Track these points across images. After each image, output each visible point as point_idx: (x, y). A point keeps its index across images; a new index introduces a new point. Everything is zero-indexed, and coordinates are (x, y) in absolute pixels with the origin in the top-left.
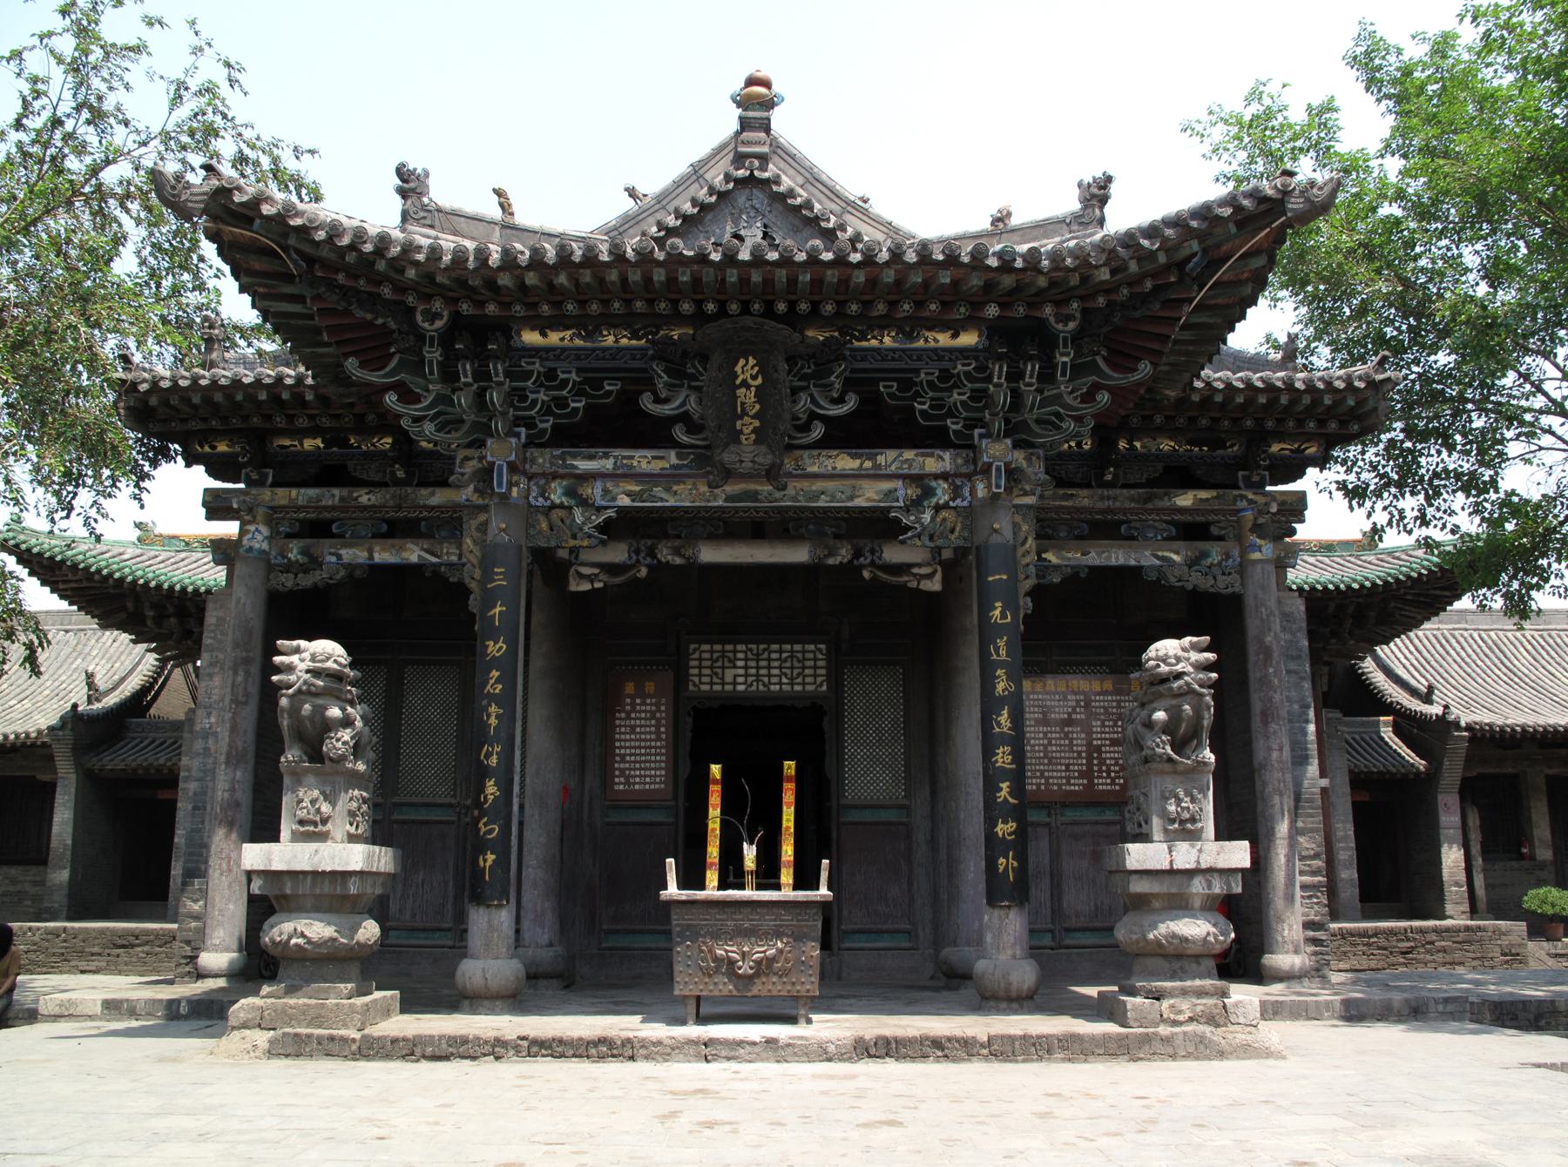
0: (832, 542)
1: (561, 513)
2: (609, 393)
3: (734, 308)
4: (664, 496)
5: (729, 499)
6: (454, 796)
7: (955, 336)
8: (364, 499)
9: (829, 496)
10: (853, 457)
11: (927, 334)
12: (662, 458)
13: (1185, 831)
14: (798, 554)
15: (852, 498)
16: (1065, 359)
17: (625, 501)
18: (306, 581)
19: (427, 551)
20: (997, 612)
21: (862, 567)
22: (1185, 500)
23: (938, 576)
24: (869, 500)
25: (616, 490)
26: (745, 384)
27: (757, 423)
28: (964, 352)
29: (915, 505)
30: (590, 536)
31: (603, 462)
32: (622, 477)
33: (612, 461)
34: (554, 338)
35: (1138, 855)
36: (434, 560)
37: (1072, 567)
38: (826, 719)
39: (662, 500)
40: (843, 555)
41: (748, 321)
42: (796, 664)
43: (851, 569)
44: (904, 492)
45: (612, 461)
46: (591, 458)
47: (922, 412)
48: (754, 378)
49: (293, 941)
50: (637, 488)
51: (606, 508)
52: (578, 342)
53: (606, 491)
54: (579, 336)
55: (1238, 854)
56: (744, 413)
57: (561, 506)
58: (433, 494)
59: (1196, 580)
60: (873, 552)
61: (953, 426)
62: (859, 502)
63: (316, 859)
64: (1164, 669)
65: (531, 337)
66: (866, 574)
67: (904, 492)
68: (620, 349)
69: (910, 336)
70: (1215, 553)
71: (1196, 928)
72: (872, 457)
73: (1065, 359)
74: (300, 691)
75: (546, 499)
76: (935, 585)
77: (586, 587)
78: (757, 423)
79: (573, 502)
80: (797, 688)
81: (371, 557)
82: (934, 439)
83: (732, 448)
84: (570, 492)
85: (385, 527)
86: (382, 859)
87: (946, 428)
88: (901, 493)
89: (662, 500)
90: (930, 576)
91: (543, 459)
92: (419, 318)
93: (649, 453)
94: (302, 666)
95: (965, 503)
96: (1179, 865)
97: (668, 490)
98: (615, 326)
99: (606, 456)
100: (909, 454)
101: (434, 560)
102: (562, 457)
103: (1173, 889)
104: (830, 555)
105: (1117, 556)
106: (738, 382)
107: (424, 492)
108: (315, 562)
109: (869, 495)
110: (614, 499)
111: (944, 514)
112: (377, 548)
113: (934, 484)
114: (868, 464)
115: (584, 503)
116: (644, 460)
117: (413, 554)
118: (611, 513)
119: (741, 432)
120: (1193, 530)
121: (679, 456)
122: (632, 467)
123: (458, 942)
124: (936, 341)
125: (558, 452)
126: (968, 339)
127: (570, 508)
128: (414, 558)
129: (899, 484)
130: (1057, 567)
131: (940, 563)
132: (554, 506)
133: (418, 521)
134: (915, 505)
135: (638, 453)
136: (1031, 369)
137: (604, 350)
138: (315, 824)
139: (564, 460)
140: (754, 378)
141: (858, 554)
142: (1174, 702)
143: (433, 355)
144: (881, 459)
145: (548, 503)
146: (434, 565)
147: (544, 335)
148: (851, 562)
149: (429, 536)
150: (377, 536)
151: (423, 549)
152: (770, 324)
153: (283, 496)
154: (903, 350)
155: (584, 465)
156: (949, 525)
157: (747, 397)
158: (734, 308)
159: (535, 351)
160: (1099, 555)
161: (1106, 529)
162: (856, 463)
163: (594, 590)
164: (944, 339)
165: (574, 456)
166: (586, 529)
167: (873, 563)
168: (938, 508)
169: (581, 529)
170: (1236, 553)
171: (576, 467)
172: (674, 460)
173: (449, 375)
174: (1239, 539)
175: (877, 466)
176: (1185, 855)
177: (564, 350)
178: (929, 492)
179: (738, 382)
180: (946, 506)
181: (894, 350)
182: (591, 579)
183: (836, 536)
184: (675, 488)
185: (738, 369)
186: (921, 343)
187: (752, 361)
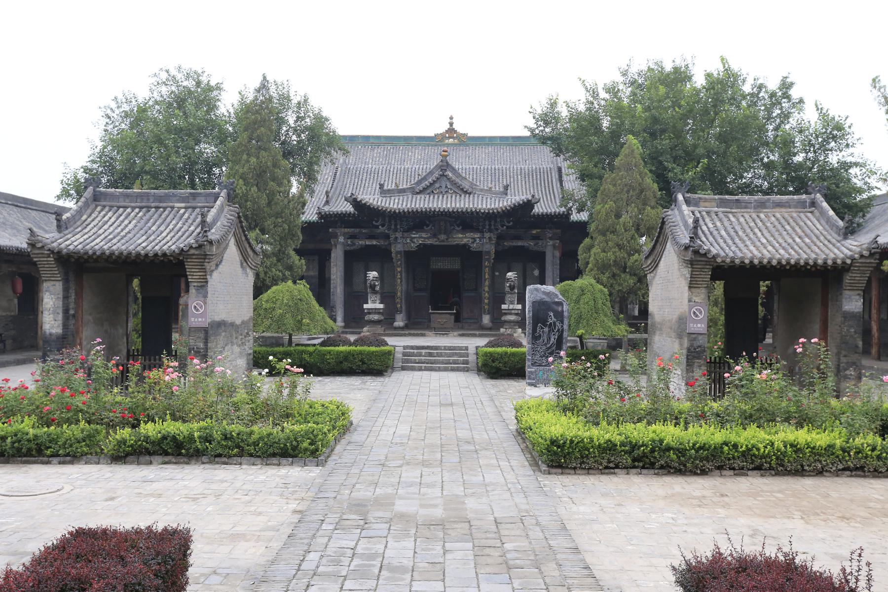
13: (512, 303)
18: (352, 248)
22: (534, 232)
35: (504, 307)
44: (471, 241)
55: (520, 307)
59: (536, 248)
67: (471, 241)
70: (540, 243)
71: (512, 318)
82: (476, 230)
86: (382, 306)
91: (406, 235)
103: (509, 312)
105: (520, 243)
108: (354, 244)
116: (424, 235)
117: (374, 242)
120: (536, 238)
123: (394, 320)
134: (473, 243)
136: (493, 223)
143: (387, 219)
153: (346, 230)
161: (518, 238)
173: (390, 221)
176: (511, 307)
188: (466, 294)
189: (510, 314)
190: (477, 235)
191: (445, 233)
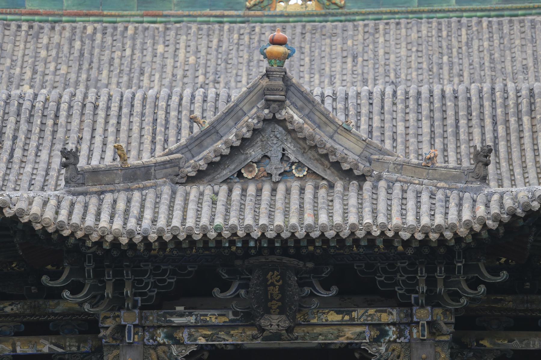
4: (226, 338)
12: (224, 315)
16: (459, 264)
19: (55, 345)
24: (348, 338)
31: (189, 318)
36: (60, 350)
39: (224, 340)
73: (459, 264)
79: (171, 342)
89: (224, 340)
101: (60, 350)
112: (18, 343)
119: (271, 308)
139: (165, 318)
151: (51, 343)
184: (232, 332)
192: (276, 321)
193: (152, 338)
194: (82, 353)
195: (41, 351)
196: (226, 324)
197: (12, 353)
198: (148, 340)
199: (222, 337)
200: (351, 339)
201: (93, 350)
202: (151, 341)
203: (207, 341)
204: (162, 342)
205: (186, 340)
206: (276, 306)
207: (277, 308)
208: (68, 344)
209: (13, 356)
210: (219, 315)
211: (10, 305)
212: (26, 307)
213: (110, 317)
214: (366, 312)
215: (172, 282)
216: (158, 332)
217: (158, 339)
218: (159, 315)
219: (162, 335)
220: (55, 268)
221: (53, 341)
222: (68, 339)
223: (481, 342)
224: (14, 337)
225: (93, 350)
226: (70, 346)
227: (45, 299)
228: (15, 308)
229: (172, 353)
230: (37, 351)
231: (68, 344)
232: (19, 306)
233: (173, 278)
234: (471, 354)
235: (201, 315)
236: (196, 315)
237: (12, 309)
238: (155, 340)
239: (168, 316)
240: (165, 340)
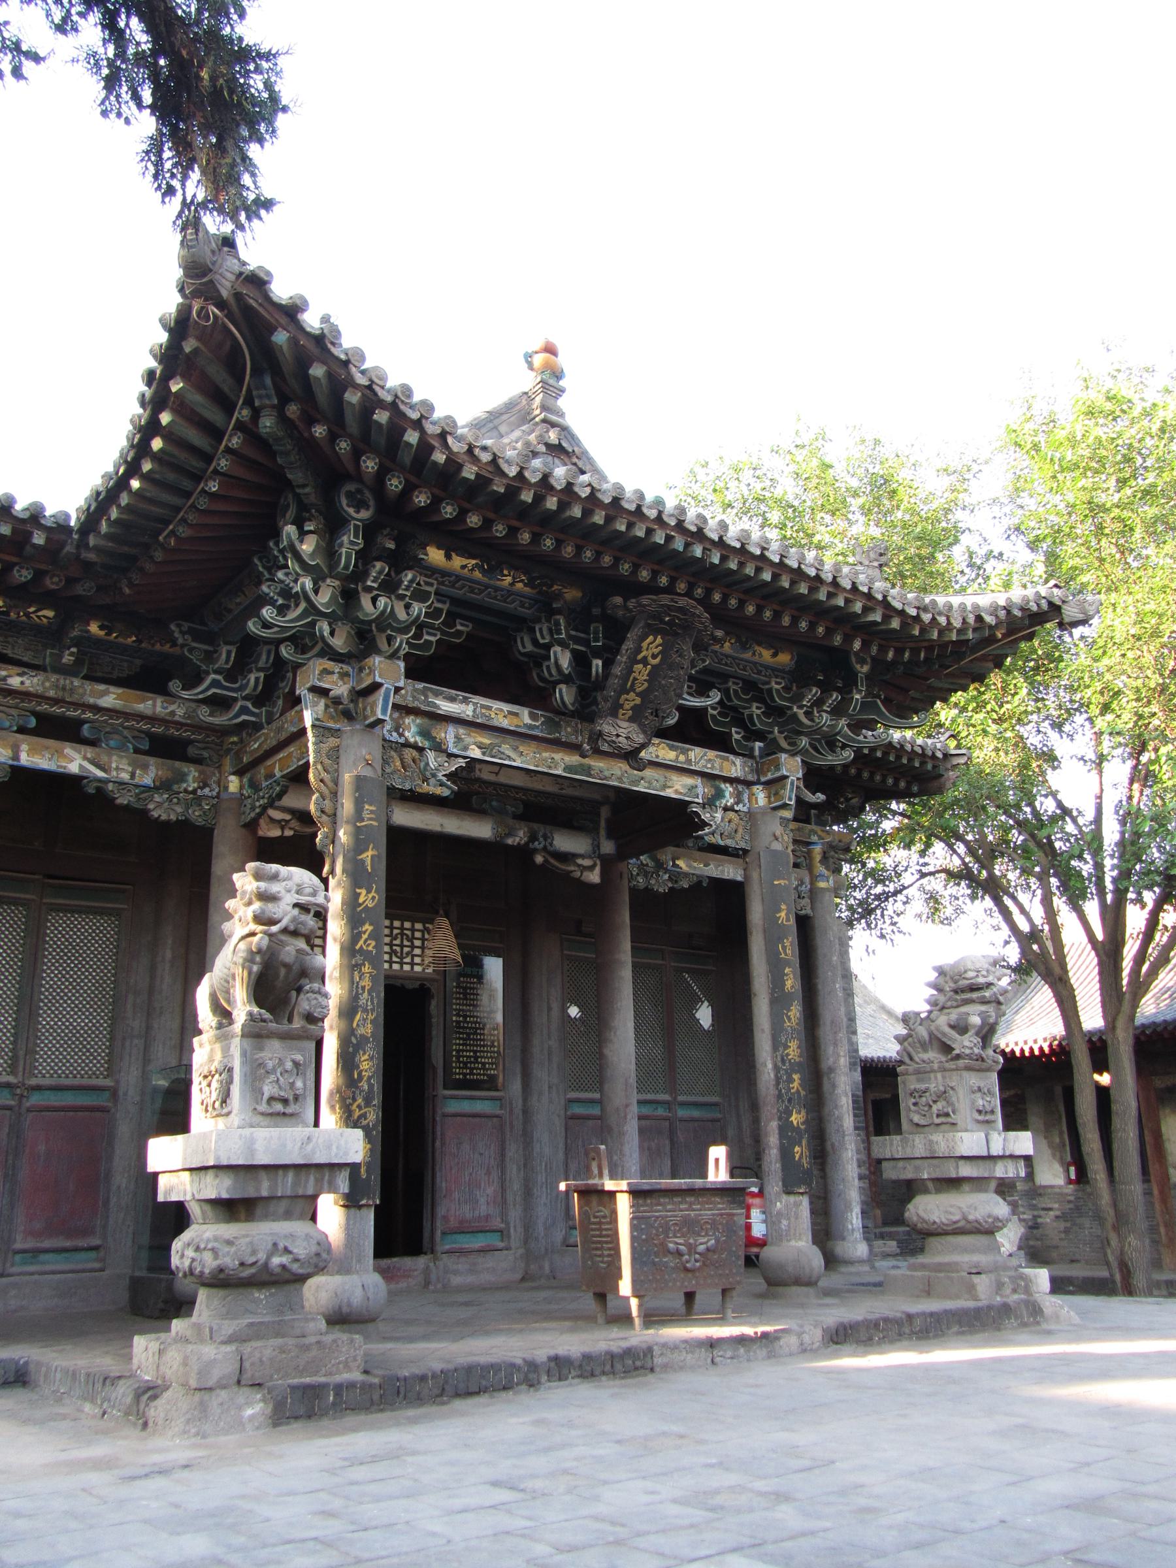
0: (511, 822)
1: (415, 753)
2: (459, 633)
3: (681, 587)
4: (513, 755)
5: (568, 768)
6: (13, 1072)
7: (775, 655)
8: (15, 682)
9: (648, 783)
10: (672, 748)
11: (757, 648)
12: (516, 714)
14: (481, 829)
15: (665, 787)
16: (858, 697)
17: (476, 753)
19: (92, 762)
20: (783, 914)
21: (535, 851)
23: (597, 870)
24: (677, 792)
25: (468, 740)
26: (644, 661)
27: (638, 701)
28: (776, 671)
29: (710, 803)
30: (442, 784)
31: (463, 707)
32: (481, 730)
33: (471, 707)
34: (457, 562)
36: (100, 774)
37: (698, 876)
38: (434, 1003)
39: (509, 758)
40: (519, 837)
41: (683, 602)
42: (406, 943)
43: (524, 853)
45: (471, 707)
46: (452, 699)
47: (713, 716)
48: (654, 656)
49: (276, 1260)
50: (487, 741)
51: (457, 756)
52: (477, 574)
53: (458, 739)
54: (479, 567)
56: (632, 689)
57: (415, 747)
58: (105, 693)
60: (545, 837)
61: (736, 735)
62: (669, 793)
63: (310, 1147)
64: (981, 980)
65: (435, 555)
66: (539, 859)
67: (702, 790)
68: (510, 593)
69: (744, 647)
72: (685, 752)
73: (858, 697)
74: (285, 931)
75: (401, 735)
76: (594, 877)
77: (276, 833)
78: (638, 701)
79: (427, 744)
80: (407, 968)
81: (16, 757)
83: (610, 720)
84: (425, 733)
85: (33, 723)
87: (730, 734)
88: (700, 790)
89: (509, 758)
90: (591, 868)
92: (344, 502)
93: (506, 707)
94: (290, 899)
95: (745, 809)
96: (994, 1153)
97: (515, 749)
98: (516, 569)
99: (465, 701)
100: (711, 754)
101: (100, 774)
102: (424, 692)
104: (509, 835)
106: (639, 657)
107: (88, 686)
109: (677, 787)
110: (466, 748)
111: (731, 814)
112: (24, 747)
113: (723, 786)
114: (682, 758)
115: (439, 748)
116: (500, 712)
118: (461, 762)
119: (621, 706)
121: (533, 716)
122: (489, 718)
124: (760, 655)
125: (420, 686)
126: (784, 658)
127: (421, 750)
128: (74, 768)
129: (698, 781)
130: (686, 875)
131: (601, 857)
132: (407, 745)
133: (81, 722)
134: (710, 803)
135: (496, 705)
137: (497, 589)
138: (285, 1101)
139: (426, 697)
140: (654, 656)
141: (533, 838)
142: (983, 1008)
144: (692, 755)
145: (402, 740)
146: (100, 780)
147: (448, 557)
148: (527, 844)
149: (92, 743)
150: (22, 730)
151: (85, 758)
152: (699, 610)
154: (734, 658)
155: (446, 707)
156: (733, 825)
157: (641, 673)
158: (681, 587)
159: (432, 571)
160: (716, 867)
162: (672, 755)
163: (282, 838)
164: (766, 655)
165: (437, 694)
166: (440, 775)
167: (545, 848)
168: (726, 809)
169: (434, 776)
170: (807, 880)
171: (438, 707)
172: (527, 720)
174: (810, 868)
175: (689, 761)
177: (459, 578)
178: (719, 794)
179: (639, 657)
180: (731, 809)
181: (727, 656)
182: (282, 824)
183: (516, 817)
184: (521, 749)
185: (645, 645)
186: (747, 655)
187: (659, 640)
188: (453, 1107)
189: (978, 1183)
190: (736, 767)
191: (636, 716)
192: (626, 731)
193: (397, 730)
194: (137, 786)
195: (65, 768)
196: (519, 730)
197: (11, 762)
198: (390, 732)
199: (507, 752)
200: (681, 793)
201: (158, 784)
202: (395, 734)
203: (484, 754)
204: (412, 740)
205: (451, 745)
206: (632, 704)
207: (632, 709)
208: (114, 765)
209: (11, 766)
210: (510, 713)
211: (19, 675)
212: (47, 684)
213: (333, 673)
214: (705, 755)
215: (431, 642)
216: (407, 721)
217: (407, 734)
218: (416, 690)
219: (414, 729)
220: (102, 633)
221: (89, 755)
222: (115, 758)
223: (677, 862)
224: (18, 735)
225: (158, 784)
226: (117, 769)
227: (86, 678)
228: (28, 683)
229: (427, 764)
230: (58, 766)
231: (114, 765)
232: (35, 680)
233: (435, 635)
234: (666, 877)
235: (483, 706)
236: (475, 704)
237: (22, 683)
238: (401, 735)
239: (430, 694)
240: (418, 739)
